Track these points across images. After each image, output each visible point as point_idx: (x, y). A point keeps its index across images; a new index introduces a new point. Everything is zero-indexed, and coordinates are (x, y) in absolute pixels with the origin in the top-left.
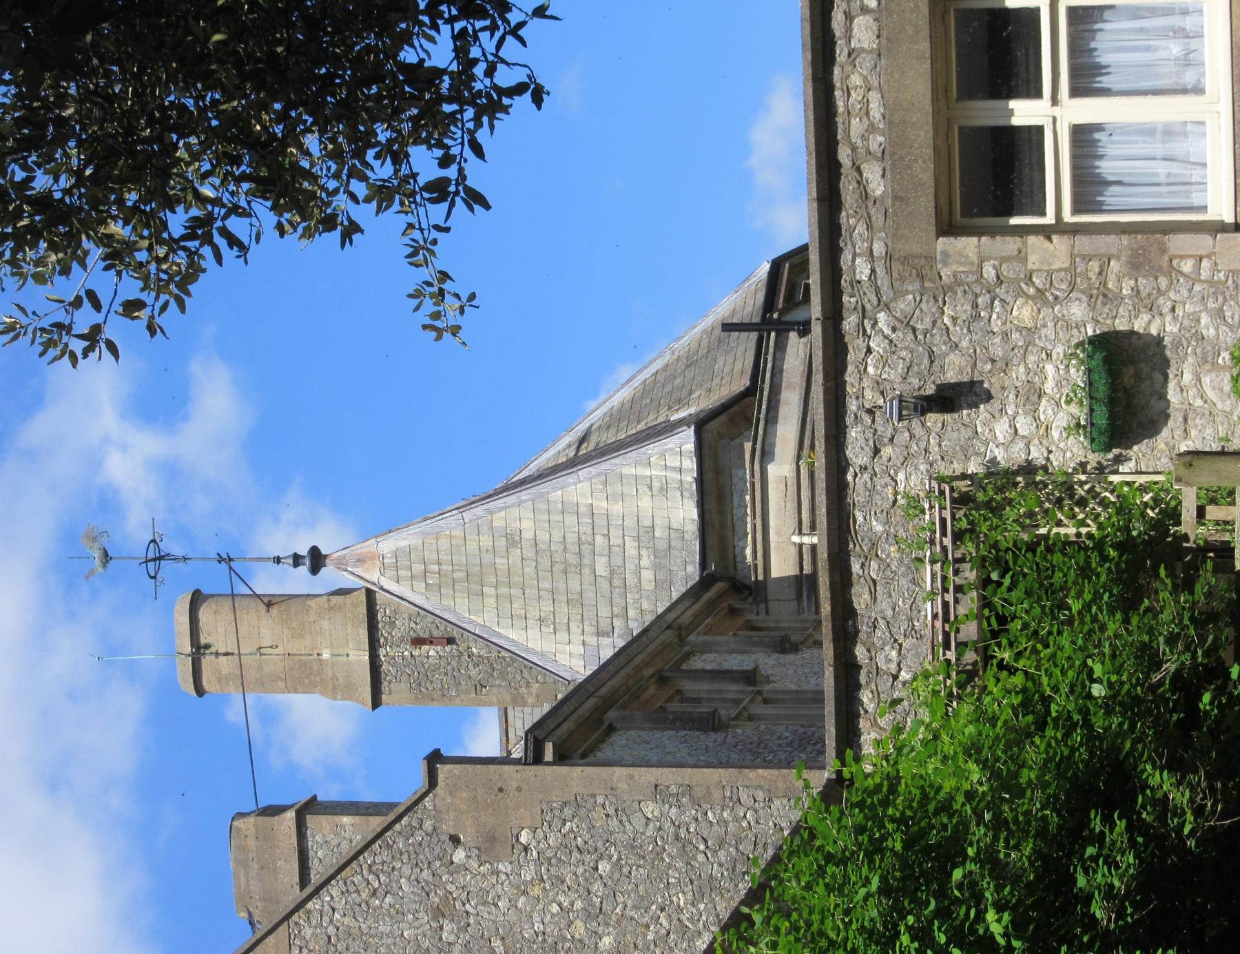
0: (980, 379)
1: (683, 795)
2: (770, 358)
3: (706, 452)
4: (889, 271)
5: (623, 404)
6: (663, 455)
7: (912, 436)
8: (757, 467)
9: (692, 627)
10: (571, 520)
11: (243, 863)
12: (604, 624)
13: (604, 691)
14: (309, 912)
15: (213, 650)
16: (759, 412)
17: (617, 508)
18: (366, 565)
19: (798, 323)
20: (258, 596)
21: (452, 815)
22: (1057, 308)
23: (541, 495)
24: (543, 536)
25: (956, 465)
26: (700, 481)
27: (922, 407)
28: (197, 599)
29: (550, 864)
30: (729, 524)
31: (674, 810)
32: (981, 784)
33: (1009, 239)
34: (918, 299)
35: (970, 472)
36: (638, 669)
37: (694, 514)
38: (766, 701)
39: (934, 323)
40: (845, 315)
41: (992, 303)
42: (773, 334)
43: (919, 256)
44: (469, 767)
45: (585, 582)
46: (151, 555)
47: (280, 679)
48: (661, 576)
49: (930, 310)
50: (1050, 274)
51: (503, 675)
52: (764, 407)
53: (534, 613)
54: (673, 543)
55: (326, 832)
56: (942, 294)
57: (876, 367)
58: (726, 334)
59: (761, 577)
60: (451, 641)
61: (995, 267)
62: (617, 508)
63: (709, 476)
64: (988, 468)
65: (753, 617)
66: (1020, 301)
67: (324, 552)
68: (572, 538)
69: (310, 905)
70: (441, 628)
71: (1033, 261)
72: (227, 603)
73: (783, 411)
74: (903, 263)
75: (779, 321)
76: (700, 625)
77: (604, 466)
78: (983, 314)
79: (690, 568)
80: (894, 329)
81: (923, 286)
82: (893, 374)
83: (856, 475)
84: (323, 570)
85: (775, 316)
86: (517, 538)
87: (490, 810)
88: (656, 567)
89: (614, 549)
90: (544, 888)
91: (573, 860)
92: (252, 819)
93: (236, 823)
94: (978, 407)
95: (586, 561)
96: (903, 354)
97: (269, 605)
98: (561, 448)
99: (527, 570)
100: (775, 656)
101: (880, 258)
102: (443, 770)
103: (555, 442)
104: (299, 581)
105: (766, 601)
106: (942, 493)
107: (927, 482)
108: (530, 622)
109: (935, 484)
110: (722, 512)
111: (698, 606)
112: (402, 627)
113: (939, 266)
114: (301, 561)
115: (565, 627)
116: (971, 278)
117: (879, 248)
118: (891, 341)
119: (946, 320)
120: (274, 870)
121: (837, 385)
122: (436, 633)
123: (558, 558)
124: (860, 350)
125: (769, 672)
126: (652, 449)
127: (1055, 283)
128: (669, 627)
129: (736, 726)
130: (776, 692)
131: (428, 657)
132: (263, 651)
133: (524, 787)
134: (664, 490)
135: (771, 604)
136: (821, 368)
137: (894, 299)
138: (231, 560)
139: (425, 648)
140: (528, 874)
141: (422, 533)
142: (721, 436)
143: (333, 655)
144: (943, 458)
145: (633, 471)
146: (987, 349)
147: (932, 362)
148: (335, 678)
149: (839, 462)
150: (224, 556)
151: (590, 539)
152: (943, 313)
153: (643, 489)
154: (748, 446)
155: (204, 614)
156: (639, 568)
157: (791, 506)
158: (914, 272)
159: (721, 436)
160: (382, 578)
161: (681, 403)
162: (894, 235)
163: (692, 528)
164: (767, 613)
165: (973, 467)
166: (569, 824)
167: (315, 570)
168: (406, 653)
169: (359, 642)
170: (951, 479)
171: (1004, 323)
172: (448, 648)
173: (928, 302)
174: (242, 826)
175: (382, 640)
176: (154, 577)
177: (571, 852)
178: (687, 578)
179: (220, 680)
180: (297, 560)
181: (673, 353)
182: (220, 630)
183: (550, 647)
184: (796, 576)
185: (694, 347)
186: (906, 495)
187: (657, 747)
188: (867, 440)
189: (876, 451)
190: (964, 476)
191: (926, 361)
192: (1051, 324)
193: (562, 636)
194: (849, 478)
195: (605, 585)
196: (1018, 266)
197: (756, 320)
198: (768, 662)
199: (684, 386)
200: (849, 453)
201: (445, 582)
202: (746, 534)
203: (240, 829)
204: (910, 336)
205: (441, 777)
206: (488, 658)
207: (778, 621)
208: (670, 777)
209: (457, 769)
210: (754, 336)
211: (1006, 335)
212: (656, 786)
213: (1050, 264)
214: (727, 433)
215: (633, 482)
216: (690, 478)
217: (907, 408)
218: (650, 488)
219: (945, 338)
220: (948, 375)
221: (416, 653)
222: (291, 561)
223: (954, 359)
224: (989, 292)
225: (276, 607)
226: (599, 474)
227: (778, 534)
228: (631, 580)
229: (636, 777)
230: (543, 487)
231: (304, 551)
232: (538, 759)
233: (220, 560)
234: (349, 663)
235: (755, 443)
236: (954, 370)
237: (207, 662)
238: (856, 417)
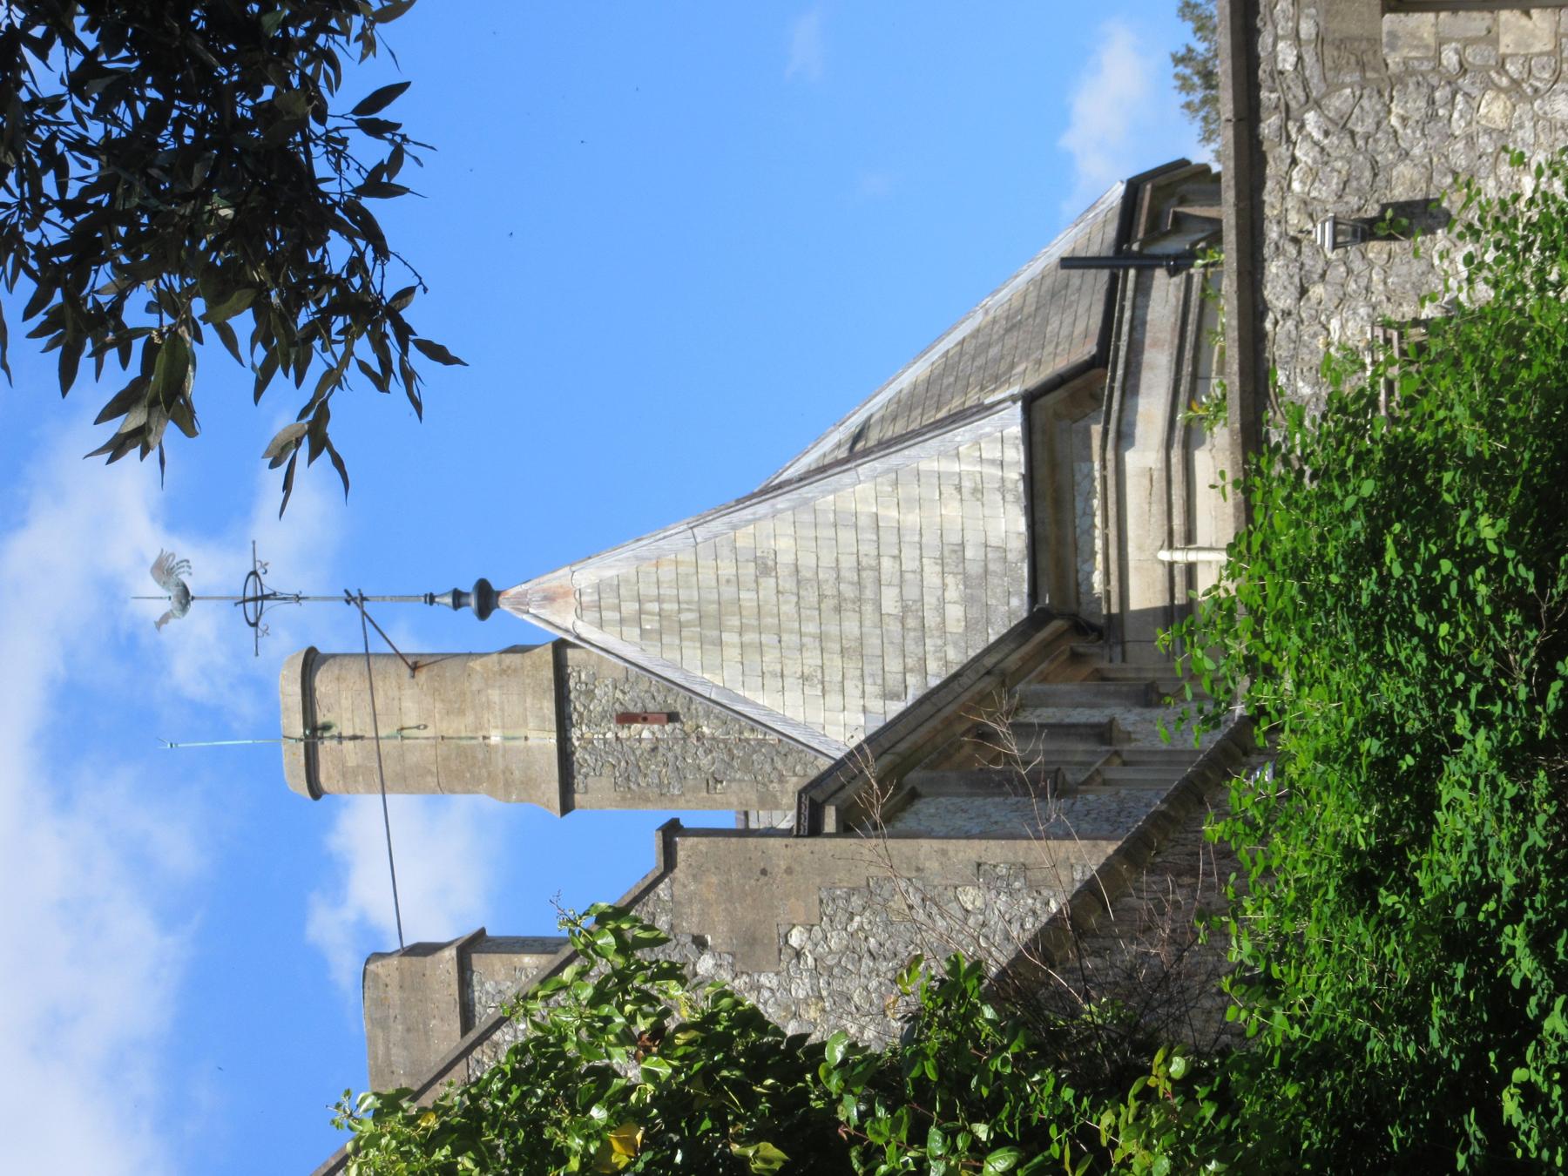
0: (1438, 196)
1: (1016, 878)
2: (1128, 304)
3: (1037, 438)
4: (1320, 59)
5: (915, 386)
6: (977, 443)
7: (1349, 272)
8: (1110, 455)
9: (1020, 674)
10: (846, 536)
11: (381, 1023)
12: (893, 681)
13: (902, 747)
14: (496, 1045)
15: (334, 731)
16: (1113, 379)
17: (912, 519)
18: (556, 605)
19: (1168, 257)
20: (401, 656)
21: (696, 907)
22: (1537, 103)
23: (805, 502)
24: (808, 560)
25: (1405, 308)
26: (1030, 478)
27: (1363, 230)
28: (312, 661)
29: (831, 975)
30: (1070, 539)
31: (1003, 897)
32: (1449, 490)
33: (1475, 14)
34: (1358, 93)
35: (1423, 317)
36: (949, 723)
37: (1021, 524)
38: (1125, 764)
39: (1378, 124)
40: (1263, 115)
41: (1454, 97)
42: (1132, 272)
43: (1360, 39)
44: (721, 842)
45: (867, 623)
46: (250, 594)
47: (429, 771)
48: (975, 612)
49: (1373, 108)
50: (1528, 59)
51: (747, 765)
52: (1120, 372)
53: (793, 668)
54: (992, 567)
55: (500, 976)
56: (1387, 85)
57: (1303, 182)
58: (1065, 272)
59: (1115, 609)
60: (672, 717)
61: (1457, 52)
62: (912, 519)
63: (1042, 472)
64: (1448, 311)
65: (1104, 665)
66: (1489, 95)
67: (495, 587)
68: (848, 562)
69: (497, 1036)
70: (660, 698)
71: (1507, 43)
72: (358, 666)
73: (1147, 377)
74: (1338, 48)
75: (1140, 255)
76: (1030, 672)
77: (895, 460)
78: (1441, 112)
79: (1015, 602)
80: (1327, 134)
81: (1363, 78)
82: (1324, 192)
83: (1276, 323)
84: (495, 613)
85: (1135, 247)
86: (771, 563)
87: (749, 901)
88: (968, 601)
89: (908, 576)
90: (823, 1010)
91: (864, 969)
92: (395, 961)
93: (371, 967)
94: (1433, 232)
95: (869, 593)
96: (1339, 164)
97: (415, 668)
98: (834, 440)
99: (784, 608)
100: (1138, 710)
101: (1309, 42)
102: (684, 846)
103: (818, 440)
104: (464, 628)
105: (1123, 643)
106: (1388, 341)
107: (1368, 329)
108: (788, 681)
109: (1379, 332)
110: (1059, 523)
111: (1027, 648)
112: (604, 696)
113: (1385, 50)
114: (463, 600)
115: (837, 688)
116: (1426, 66)
117: (1307, 29)
118: (1323, 149)
119: (1394, 121)
120: (426, 1033)
121: (1252, 207)
122: (651, 706)
123: (829, 590)
124: (1282, 161)
125: (1130, 729)
126: (962, 435)
127: (1535, 71)
128: (988, 673)
129: (1086, 792)
130: (1141, 752)
131: (640, 740)
132: (405, 733)
133: (798, 868)
134: (978, 492)
135: (1129, 647)
136: (1232, 183)
137: (1327, 95)
138: (363, 599)
139: (636, 727)
140: (800, 990)
141: (637, 558)
142: (1058, 416)
143: (506, 738)
144: (1389, 299)
145: (935, 466)
146: (1446, 157)
147: (1375, 175)
148: (507, 770)
149: (1255, 306)
150: (355, 594)
151: (874, 563)
152: (1389, 112)
153: (949, 490)
154: (1097, 430)
155: (324, 683)
156: (942, 601)
157: (1158, 509)
158: (1353, 59)
159: (1058, 416)
160: (579, 623)
161: (998, 380)
162: (1327, 11)
163: (1017, 543)
164: (1124, 660)
165: (1428, 312)
166: (857, 919)
167: (484, 611)
168: (609, 735)
169: (543, 719)
170: (1401, 327)
171: (1469, 124)
172: (668, 728)
173: (1370, 97)
174: (381, 971)
175: (575, 717)
176: (255, 625)
177: (860, 959)
178: (1011, 613)
179: (344, 776)
180: (458, 598)
181: (986, 313)
182: (346, 703)
183: (816, 716)
184: (1165, 608)
185: (1016, 304)
186: (1342, 346)
187: (978, 816)
188: (1291, 277)
189: (1303, 291)
190: (1416, 322)
191: (1368, 174)
192: (1528, 124)
193: (834, 699)
194: (1268, 325)
195: (894, 627)
196: (1486, 50)
197: (1107, 251)
198: (1128, 718)
199: (1002, 357)
200: (1268, 294)
201: (669, 627)
202: (1093, 554)
203: (377, 975)
204: (1347, 142)
205: (681, 855)
206: (725, 742)
207: (1139, 670)
208: (996, 851)
209: (703, 843)
210: (1105, 275)
211: (1470, 140)
212: (979, 865)
213: (1529, 46)
214: (1067, 415)
215: (935, 481)
216: (1015, 474)
217: (1343, 233)
218: (959, 489)
219: (1392, 144)
220: (1396, 192)
221: (623, 734)
222: (449, 600)
223: (1404, 171)
224: (1449, 83)
225: (424, 670)
226: (888, 471)
227: (1140, 548)
228: (931, 620)
229: (951, 853)
230: (807, 491)
231: (468, 586)
232: (811, 826)
233: (349, 599)
234: (528, 750)
235: (1107, 422)
236: (1404, 185)
237: (326, 748)
238: (1277, 248)
